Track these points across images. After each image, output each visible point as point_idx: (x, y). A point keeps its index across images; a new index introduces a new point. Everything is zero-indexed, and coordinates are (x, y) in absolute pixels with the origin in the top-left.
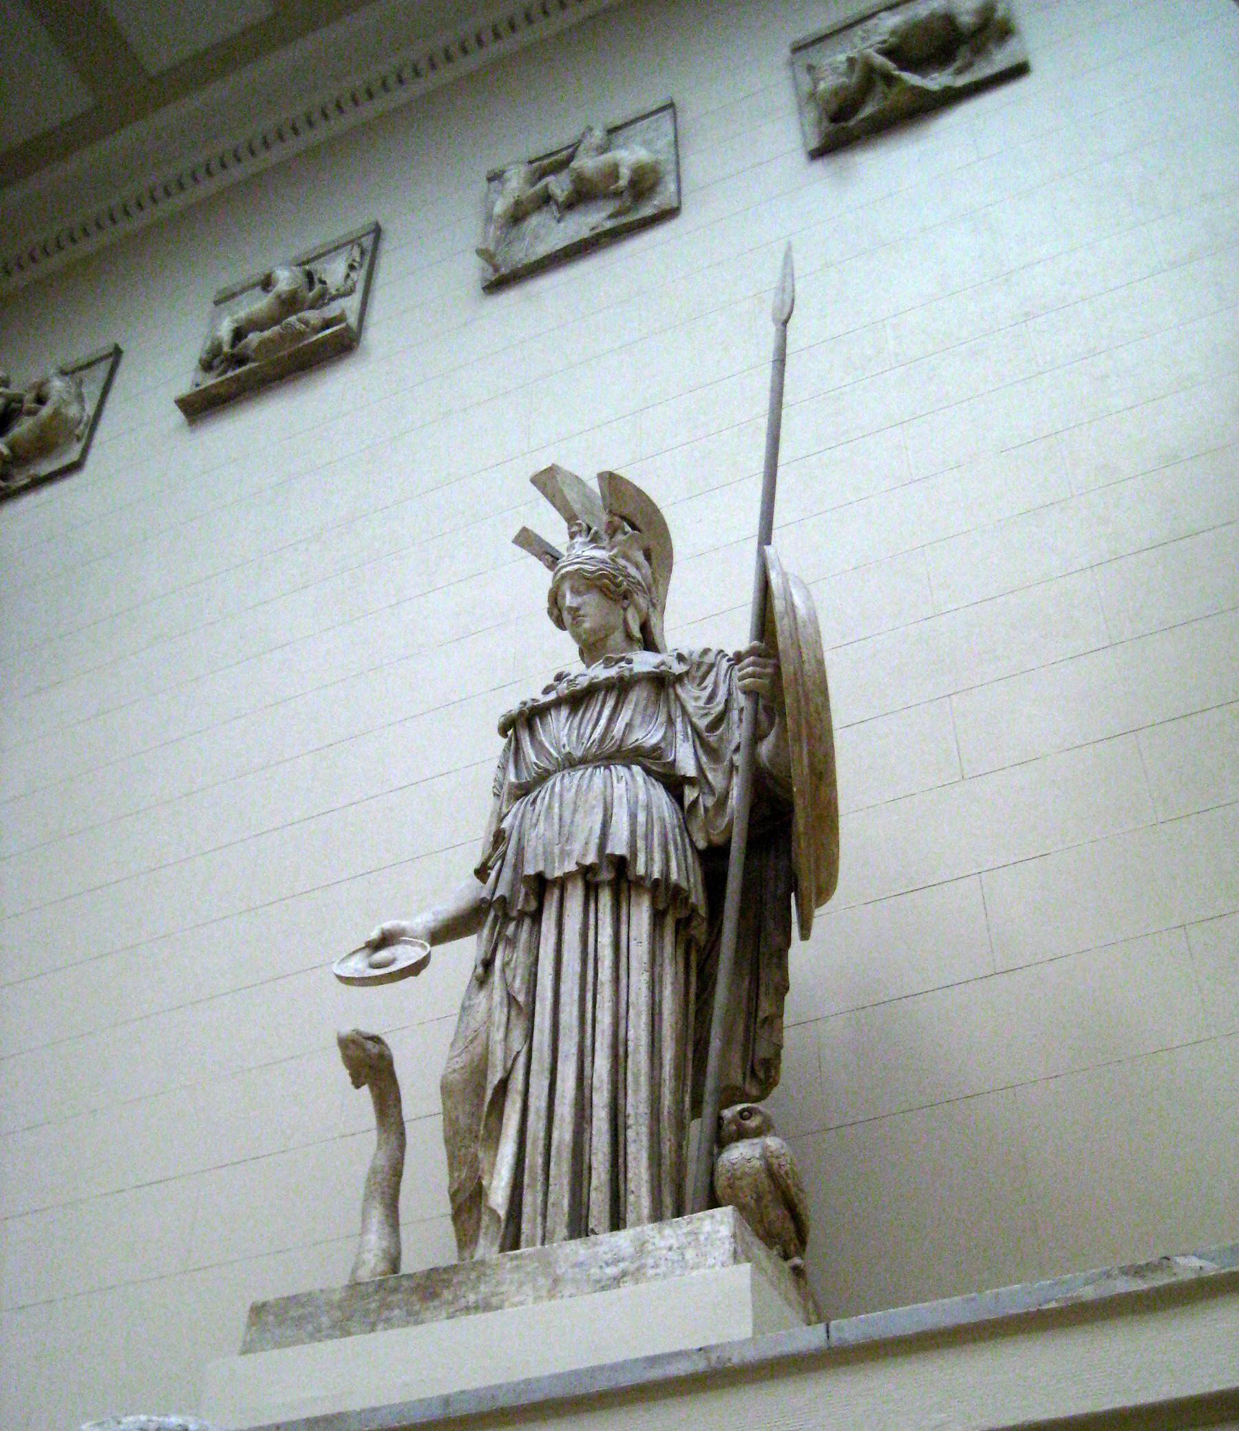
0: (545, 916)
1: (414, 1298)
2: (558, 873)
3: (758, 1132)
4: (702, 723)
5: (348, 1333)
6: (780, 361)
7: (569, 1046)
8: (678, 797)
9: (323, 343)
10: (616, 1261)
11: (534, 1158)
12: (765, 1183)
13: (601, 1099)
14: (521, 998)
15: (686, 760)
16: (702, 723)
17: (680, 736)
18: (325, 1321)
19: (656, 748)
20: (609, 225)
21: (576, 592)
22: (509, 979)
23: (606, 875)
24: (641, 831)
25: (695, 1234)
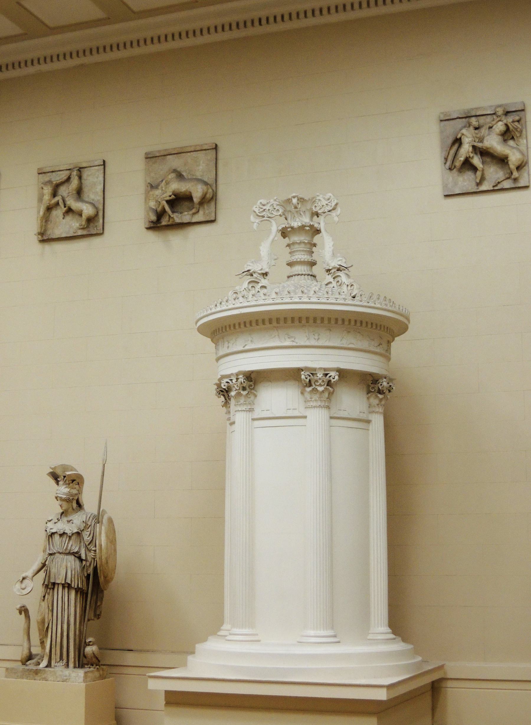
5: (23, 678)
10: (66, 676)
11: (54, 643)
13: (65, 634)
16: (87, 544)
23: (66, 585)
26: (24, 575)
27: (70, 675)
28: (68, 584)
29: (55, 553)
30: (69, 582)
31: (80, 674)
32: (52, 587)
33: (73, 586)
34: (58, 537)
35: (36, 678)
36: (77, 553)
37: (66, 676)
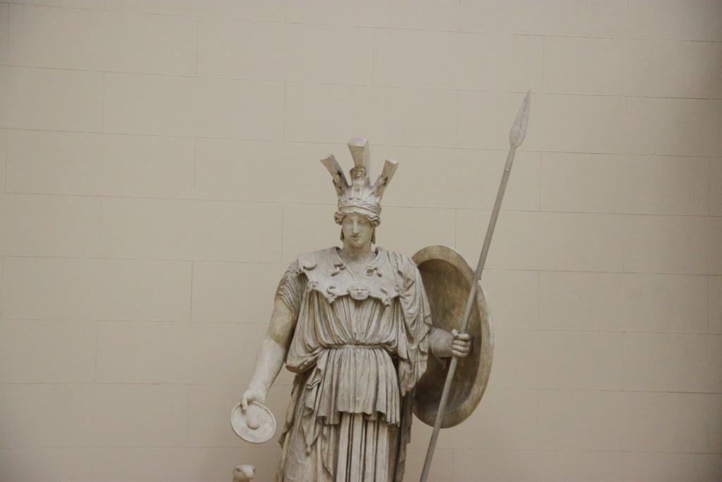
0: (342, 429)
2: (351, 411)
4: (409, 322)
8: (397, 366)
14: (332, 473)
15: (403, 349)
17: (400, 329)
21: (359, 222)
22: (325, 459)
26: (248, 394)
28: (310, 409)
29: (344, 344)
30: (383, 411)
32: (337, 422)
33: (388, 420)
34: (352, 306)
36: (389, 344)
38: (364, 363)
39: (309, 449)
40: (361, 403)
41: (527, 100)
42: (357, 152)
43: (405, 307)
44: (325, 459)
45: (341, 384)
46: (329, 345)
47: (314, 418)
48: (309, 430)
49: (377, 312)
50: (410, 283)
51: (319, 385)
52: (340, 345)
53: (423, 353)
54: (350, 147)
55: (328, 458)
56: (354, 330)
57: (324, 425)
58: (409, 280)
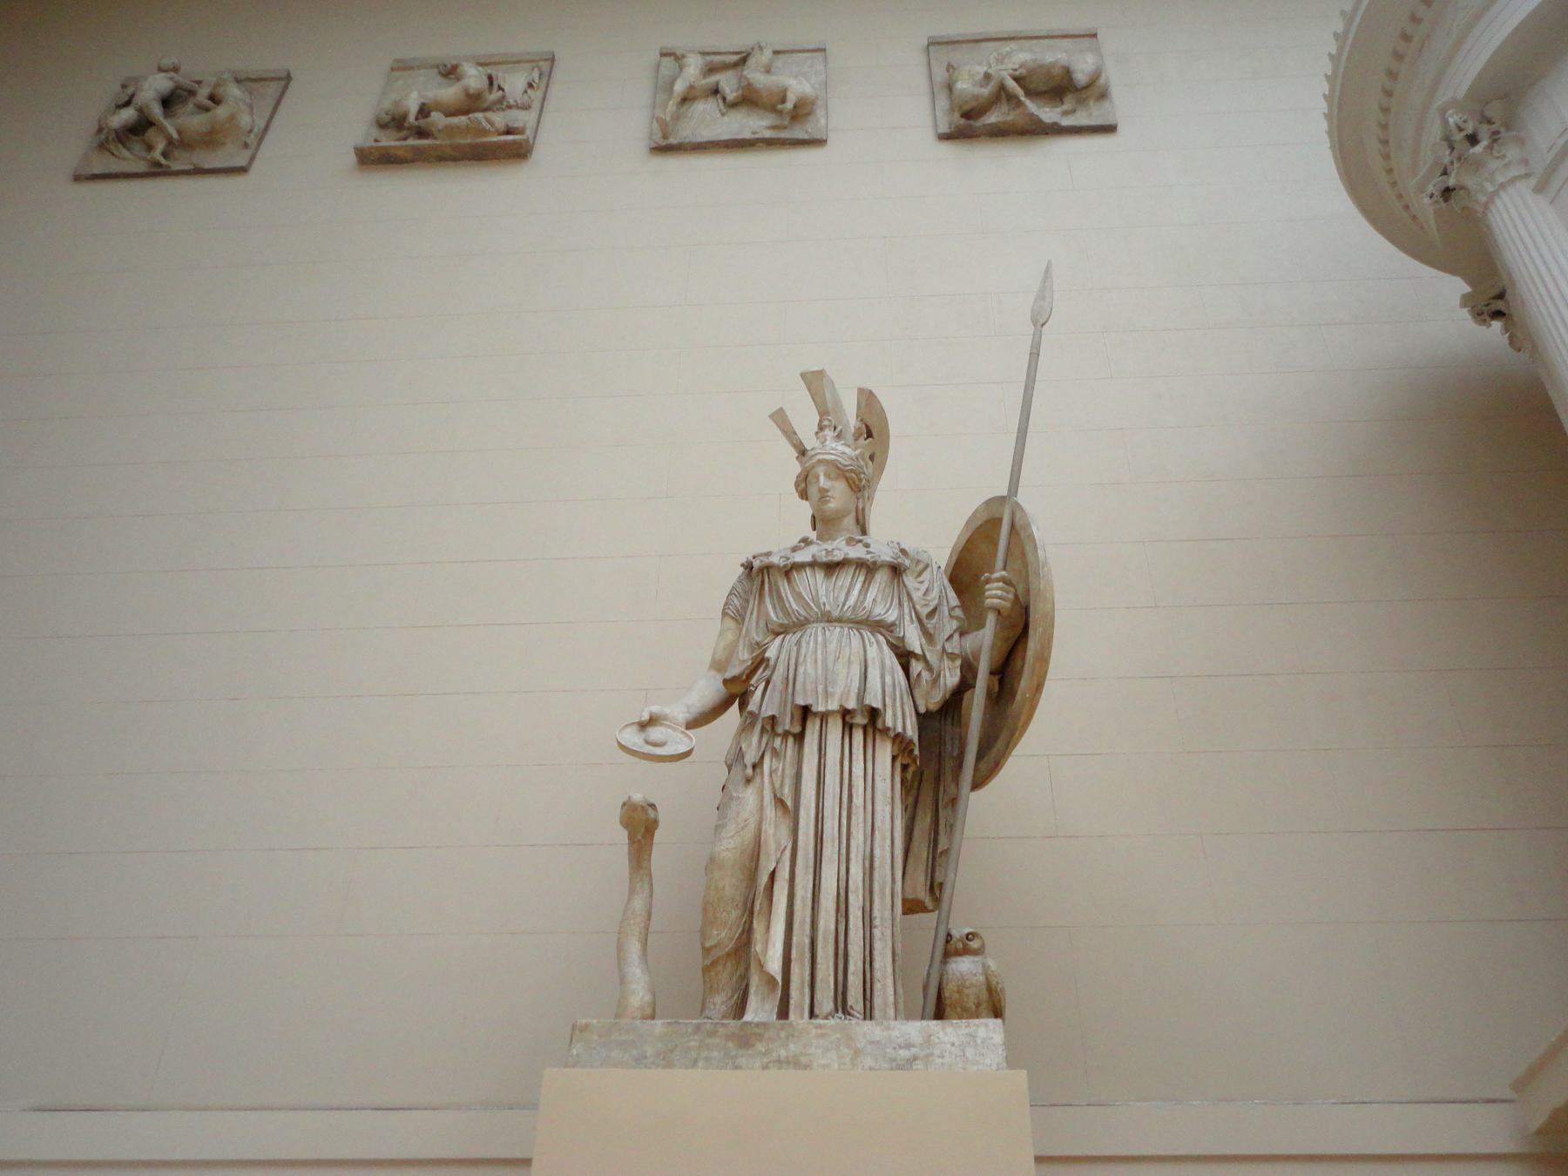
1: (730, 1044)
2: (821, 708)
3: (976, 952)
5: (670, 1065)
6: (1035, 355)
7: (830, 851)
9: (499, 145)
10: (909, 1046)
11: (801, 938)
12: (984, 995)
14: (789, 803)
16: (924, 612)
17: (907, 618)
18: (650, 1051)
19: (893, 624)
20: (768, 134)
21: (828, 476)
22: (777, 785)
23: (860, 720)
24: (888, 690)
25: (973, 1036)
27: (928, 1039)
30: (877, 704)
31: (982, 1032)
32: (797, 729)
34: (820, 575)
35: (742, 1061)
37: (909, 1046)
38: (840, 642)
39: (749, 771)
40: (837, 697)
41: (1047, 270)
42: (815, 382)
43: (917, 596)
44: (777, 785)
45: (801, 670)
46: (781, 625)
47: (758, 728)
48: (749, 745)
49: (861, 579)
50: (921, 566)
51: (768, 683)
52: (801, 624)
53: (952, 657)
54: (803, 376)
55: (782, 785)
56: (823, 599)
57: (774, 733)
58: (918, 562)
